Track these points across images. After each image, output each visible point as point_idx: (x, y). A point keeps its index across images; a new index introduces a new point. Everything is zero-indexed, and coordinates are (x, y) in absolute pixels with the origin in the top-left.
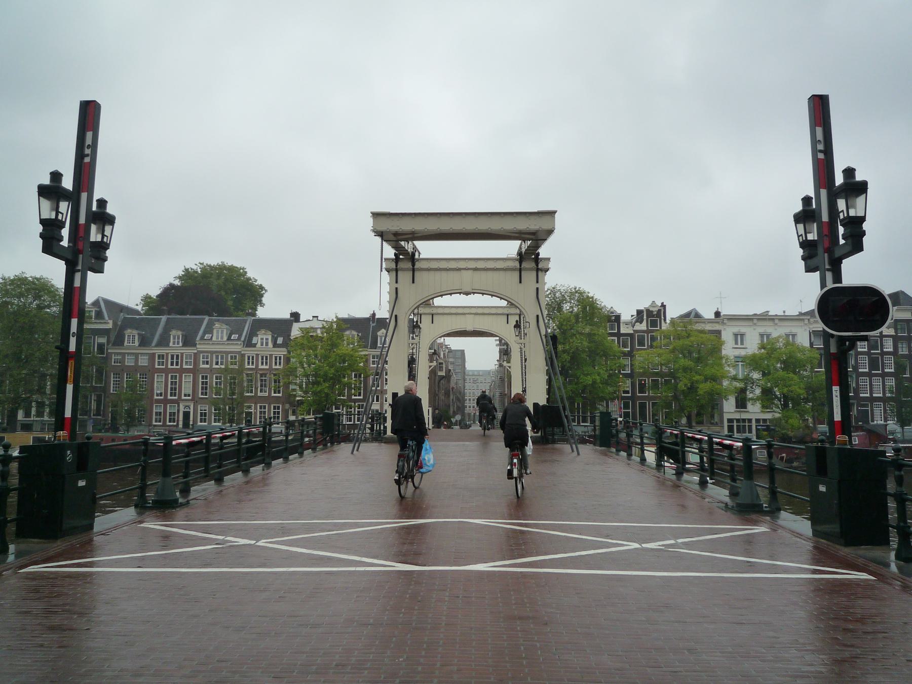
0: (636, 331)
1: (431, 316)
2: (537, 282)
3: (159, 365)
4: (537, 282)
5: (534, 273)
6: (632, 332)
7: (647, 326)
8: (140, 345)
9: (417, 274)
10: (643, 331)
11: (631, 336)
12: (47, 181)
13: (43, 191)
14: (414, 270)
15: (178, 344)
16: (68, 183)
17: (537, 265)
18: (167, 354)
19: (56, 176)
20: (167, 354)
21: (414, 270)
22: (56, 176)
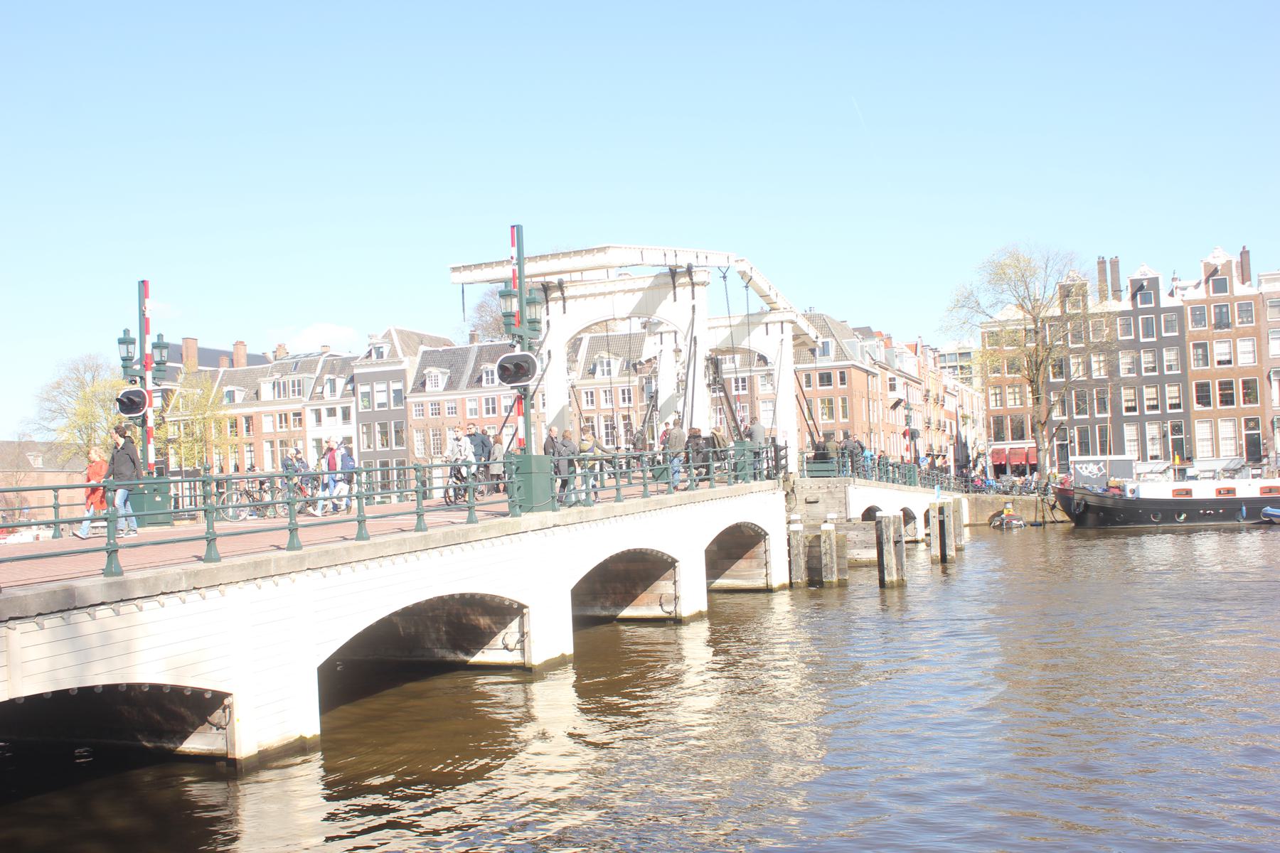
0: (1189, 302)
1: (673, 334)
2: (693, 298)
3: (471, 414)
4: (693, 298)
5: (690, 288)
6: (1181, 304)
7: (1207, 292)
8: (445, 389)
9: (569, 303)
10: (1202, 301)
11: (1179, 311)
12: (122, 336)
13: (121, 342)
14: (564, 299)
15: (493, 382)
16: (135, 334)
17: (691, 279)
18: (480, 398)
19: (126, 332)
20: (480, 398)
21: (564, 299)
22: (126, 332)
